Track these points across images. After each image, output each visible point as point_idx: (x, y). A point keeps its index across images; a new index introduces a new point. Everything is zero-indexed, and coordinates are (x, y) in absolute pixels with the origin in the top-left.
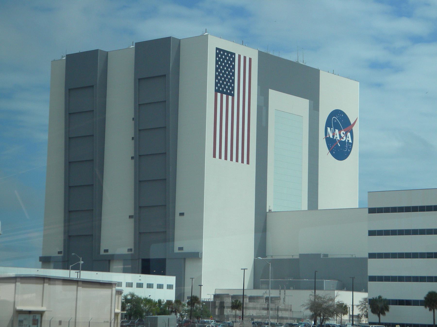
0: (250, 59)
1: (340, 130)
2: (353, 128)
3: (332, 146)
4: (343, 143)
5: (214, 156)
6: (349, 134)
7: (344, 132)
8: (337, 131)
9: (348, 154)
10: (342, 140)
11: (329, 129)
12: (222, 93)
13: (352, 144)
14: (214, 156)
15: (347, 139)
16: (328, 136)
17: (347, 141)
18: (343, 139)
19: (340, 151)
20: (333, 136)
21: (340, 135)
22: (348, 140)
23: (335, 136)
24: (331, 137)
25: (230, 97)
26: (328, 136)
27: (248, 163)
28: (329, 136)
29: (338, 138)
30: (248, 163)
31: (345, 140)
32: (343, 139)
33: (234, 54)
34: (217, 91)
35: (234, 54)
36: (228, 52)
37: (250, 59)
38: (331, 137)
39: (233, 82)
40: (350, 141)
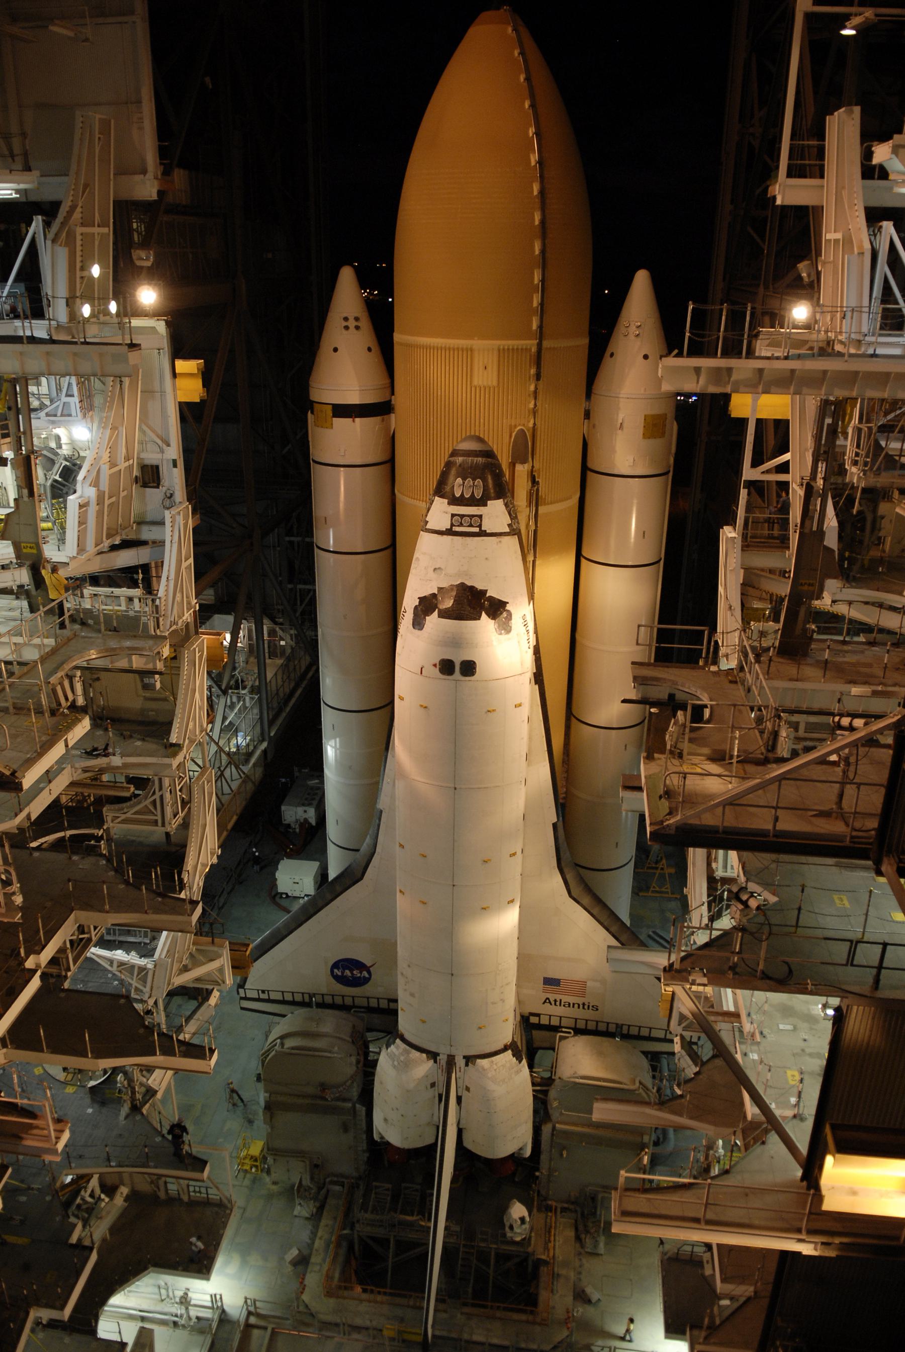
1: (351, 971)
21: (352, 974)
38: (339, 974)
40: (367, 975)
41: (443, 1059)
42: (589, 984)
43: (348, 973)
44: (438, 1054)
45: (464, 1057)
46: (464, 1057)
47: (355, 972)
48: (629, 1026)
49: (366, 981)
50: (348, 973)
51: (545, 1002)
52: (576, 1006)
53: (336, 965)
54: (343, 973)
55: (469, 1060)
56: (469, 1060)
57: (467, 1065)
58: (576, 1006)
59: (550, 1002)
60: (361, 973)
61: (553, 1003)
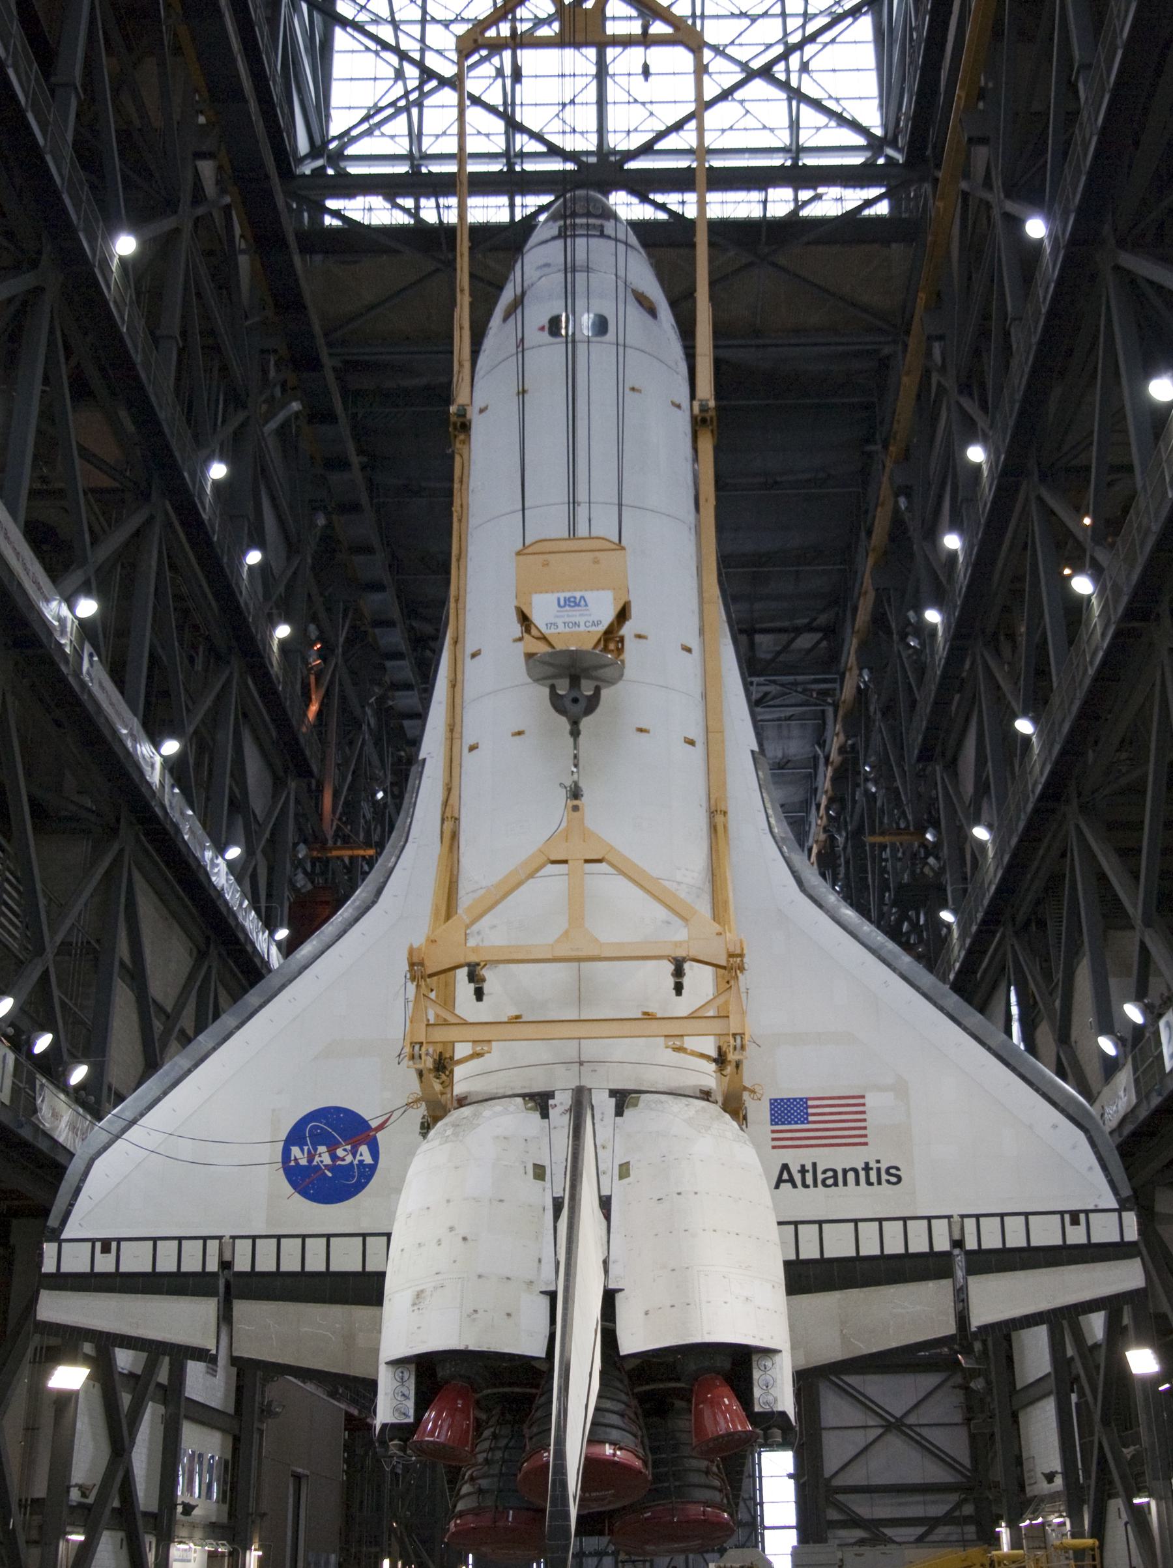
2: (379, 1135)
3: (302, 1180)
6: (364, 1149)
7: (348, 1147)
9: (359, 1187)
10: (339, 1163)
13: (373, 1168)
15: (358, 1158)
16: (292, 1163)
17: (356, 1162)
18: (343, 1160)
20: (310, 1160)
21: (334, 1157)
22: (361, 1162)
23: (317, 1159)
26: (292, 1163)
28: (297, 1163)
29: (327, 1160)
31: (352, 1163)
32: (343, 1160)
40: (368, 1160)
41: (562, 1101)
42: (871, 1100)
43: (323, 1157)
44: (550, 1095)
45: (613, 1093)
46: (613, 1093)
47: (340, 1152)
48: (978, 1217)
49: (367, 1173)
50: (323, 1157)
51: (780, 1181)
52: (851, 1176)
53: (296, 1136)
54: (311, 1159)
55: (623, 1099)
56: (623, 1099)
57: (619, 1112)
58: (851, 1176)
59: (791, 1180)
61: (798, 1178)
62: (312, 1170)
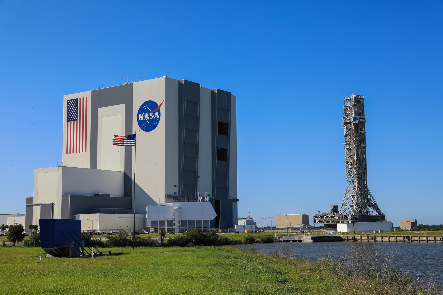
0: (86, 98)
4: (151, 121)
5: (67, 153)
6: (157, 113)
8: (147, 114)
9: (156, 126)
11: (140, 115)
12: (71, 121)
13: (159, 119)
14: (67, 153)
18: (151, 117)
19: (148, 126)
20: (144, 118)
21: (149, 117)
24: (142, 119)
25: (75, 121)
27: (86, 151)
29: (148, 118)
30: (86, 151)
32: (151, 117)
33: (77, 99)
34: (68, 121)
35: (77, 99)
36: (74, 100)
37: (86, 98)
38: (142, 119)
39: (77, 113)
40: (158, 117)
47: (151, 115)
49: (158, 120)
53: (140, 112)
60: (154, 115)
62: (144, 121)
